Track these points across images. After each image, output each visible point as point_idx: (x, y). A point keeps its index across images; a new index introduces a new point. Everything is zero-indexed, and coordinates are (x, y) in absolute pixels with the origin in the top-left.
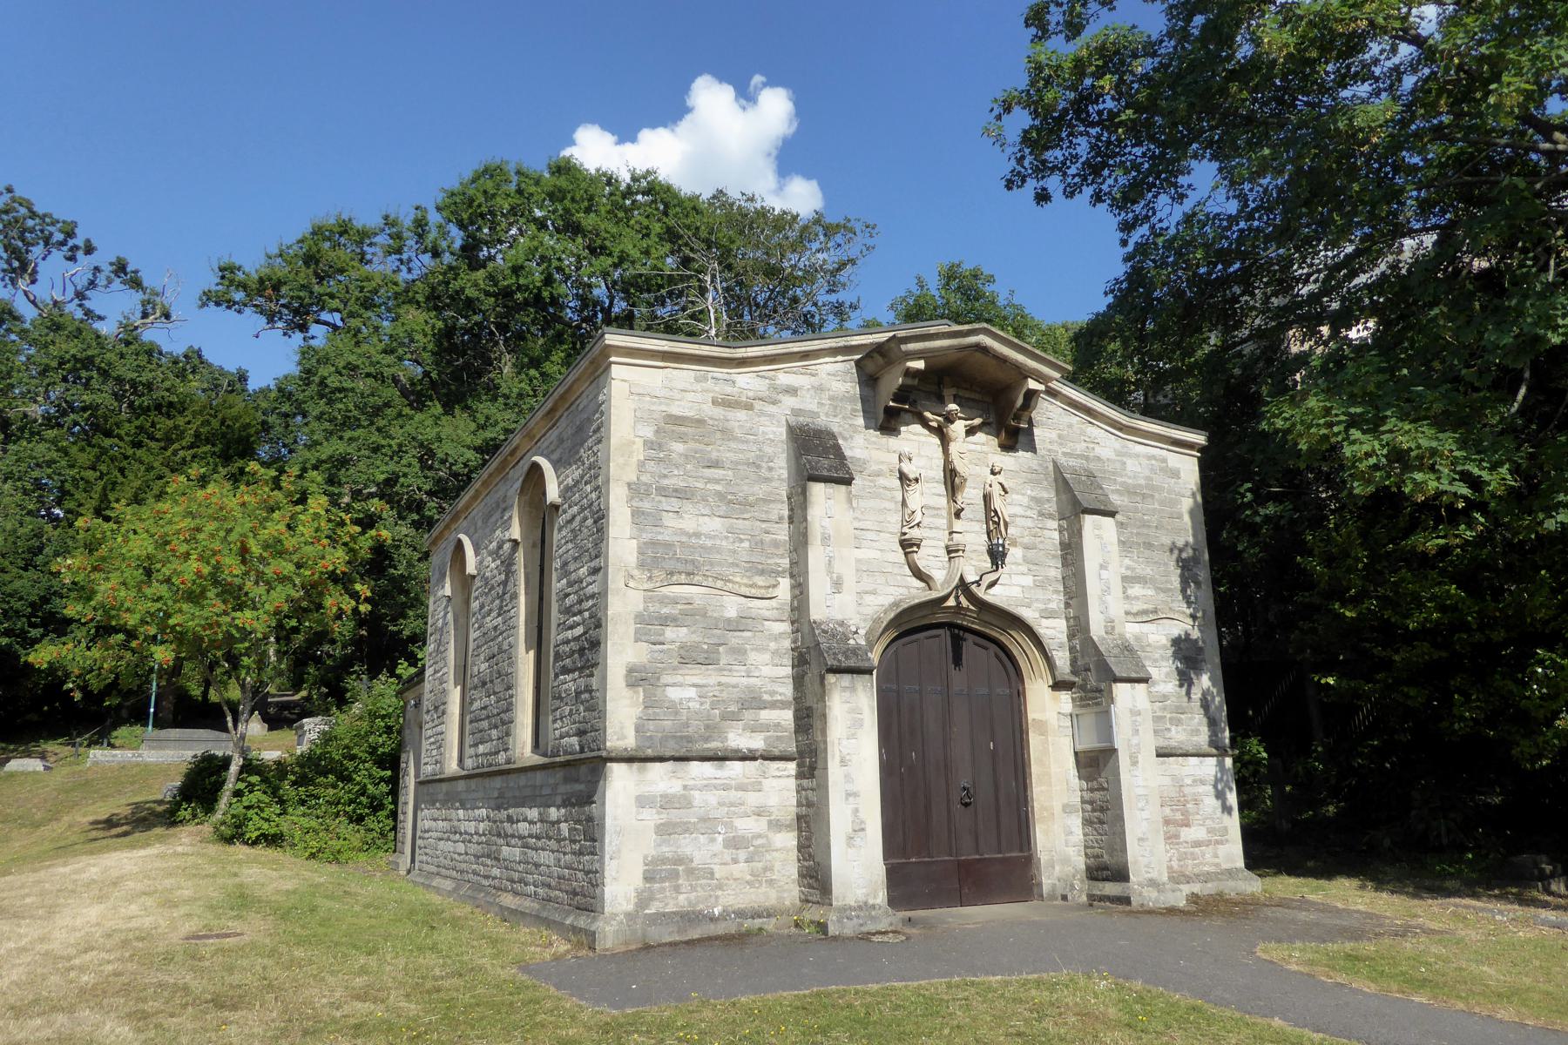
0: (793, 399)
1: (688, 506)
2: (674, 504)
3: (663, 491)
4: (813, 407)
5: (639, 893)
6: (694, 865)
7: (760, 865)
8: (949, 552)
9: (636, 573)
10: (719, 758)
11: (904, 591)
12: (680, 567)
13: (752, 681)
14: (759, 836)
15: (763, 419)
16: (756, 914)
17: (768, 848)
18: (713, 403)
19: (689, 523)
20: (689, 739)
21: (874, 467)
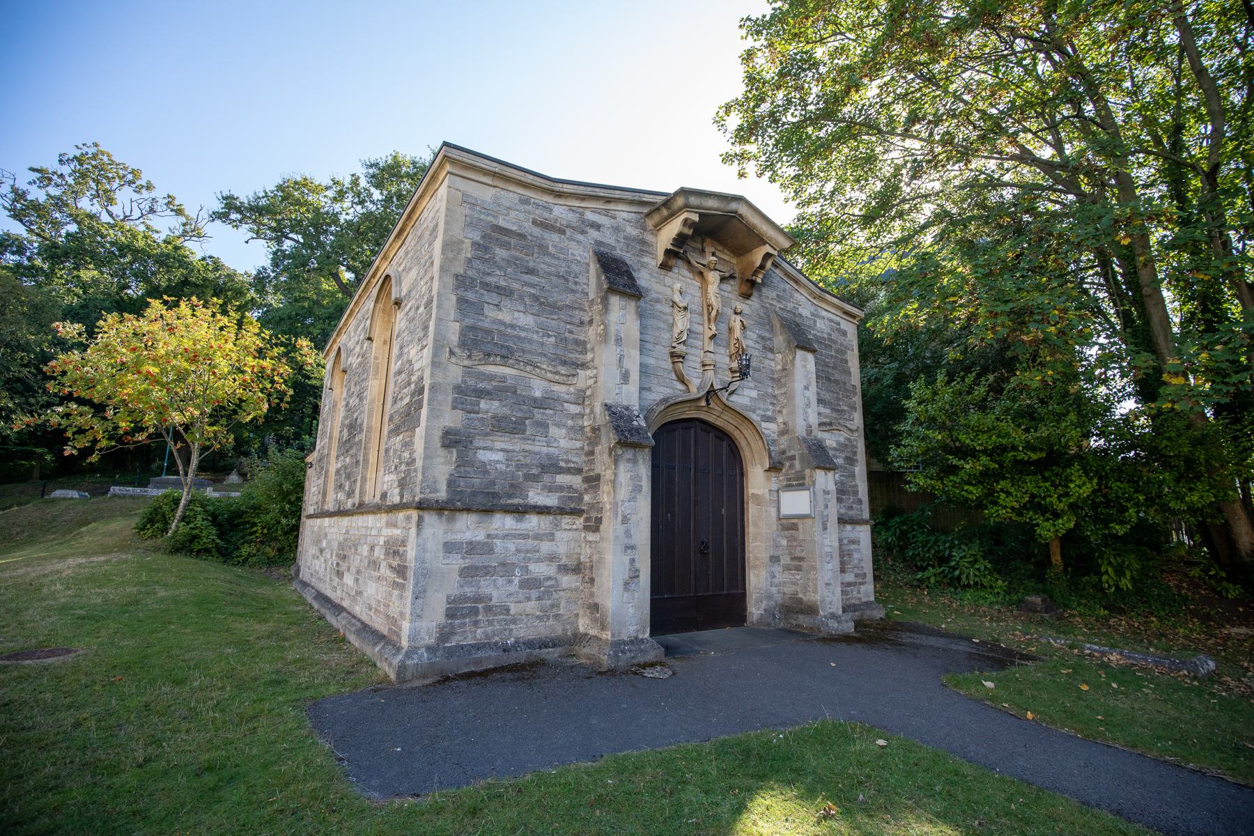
0: (597, 233)
1: (506, 302)
2: (494, 298)
3: (485, 285)
4: (612, 242)
5: (441, 628)
6: (492, 603)
7: (548, 602)
8: (704, 365)
9: (457, 350)
10: (521, 511)
11: (669, 391)
12: (496, 350)
13: (551, 450)
14: (549, 578)
15: (572, 243)
16: (544, 644)
17: (556, 587)
18: (533, 223)
19: (505, 316)
20: (495, 495)
21: (654, 295)
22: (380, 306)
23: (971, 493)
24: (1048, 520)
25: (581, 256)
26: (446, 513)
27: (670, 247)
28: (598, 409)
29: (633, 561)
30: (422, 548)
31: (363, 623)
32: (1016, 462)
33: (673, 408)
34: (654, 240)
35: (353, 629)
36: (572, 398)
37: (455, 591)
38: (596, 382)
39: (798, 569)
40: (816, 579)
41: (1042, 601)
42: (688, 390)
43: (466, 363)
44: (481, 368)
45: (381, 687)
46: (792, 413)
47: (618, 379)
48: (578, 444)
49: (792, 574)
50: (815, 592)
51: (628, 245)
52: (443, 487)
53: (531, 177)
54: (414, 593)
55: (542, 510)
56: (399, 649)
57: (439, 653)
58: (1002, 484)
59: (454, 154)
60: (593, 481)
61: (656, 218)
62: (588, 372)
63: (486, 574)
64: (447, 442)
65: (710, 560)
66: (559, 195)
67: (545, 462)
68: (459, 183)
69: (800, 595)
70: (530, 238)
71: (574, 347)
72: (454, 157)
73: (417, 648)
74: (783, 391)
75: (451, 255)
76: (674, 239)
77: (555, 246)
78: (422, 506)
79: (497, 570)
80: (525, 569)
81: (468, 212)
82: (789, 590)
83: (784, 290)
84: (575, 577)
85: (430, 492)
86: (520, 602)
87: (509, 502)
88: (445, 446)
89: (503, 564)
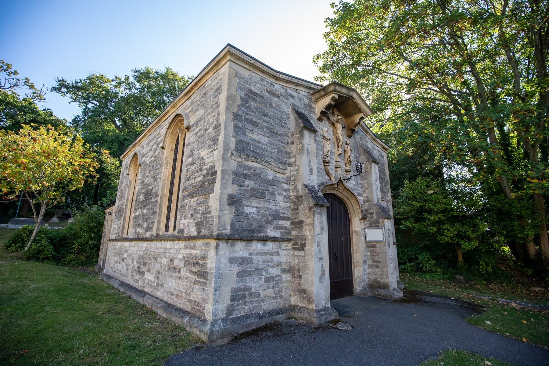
0: (292, 100)
1: (256, 129)
2: (250, 127)
3: (247, 120)
4: (298, 105)
5: (228, 307)
6: (252, 291)
7: (277, 289)
8: (336, 168)
9: (234, 152)
10: (264, 240)
11: (323, 179)
12: (252, 154)
13: (277, 207)
14: (277, 276)
15: (283, 103)
16: (277, 313)
17: (281, 281)
19: (255, 137)
20: (252, 231)
22: (170, 131)
23: (433, 230)
24: (466, 242)
25: (287, 110)
26: (230, 241)
27: (324, 110)
28: (300, 187)
29: (322, 266)
30: (219, 262)
31: (165, 302)
32: (453, 216)
33: (327, 187)
34: (315, 106)
35: (159, 306)
36: (285, 181)
37: (235, 286)
38: (297, 173)
39: (377, 267)
40: (388, 271)
41: (464, 278)
42: (330, 180)
43: (239, 159)
44: (246, 163)
45: (199, 346)
46: (371, 192)
47: (309, 172)
48: (288, 205)
49: (374, 269)
50: (387, 277)
51: (305, 108)
52: (228, 227)
53: (266, 68)
54: (215, 288)
55: (274, 240)
56: (205, 321)
57: (229, 322)
58: (445, 226)
59: (233, 51)
60: (298, 224)
61: (317, 95)
62: (292, 168)
63: (249, 275)
64: (230, 202)
65: (339, 263)
66: (277, 79)
67: (275, 214)
68: (234, 66)
69: (379, 279)
70: (265, 98)
71: (285, 155)
72: (233, 52)
73: (217, 320)
74: (366, 182)
75: (231, 102)
76: (326, 106)
77: (276, 104)
78: (219, 238)
79: (254, 273)
80: (267, 272)
81: (238, 81)
82: (372, 277)
83: (362, 135)
84: (289, 275)
85: (223, 230)
86: (265, 290)
87: (259, 235)
88: (229, 204)
89: (257, 269)
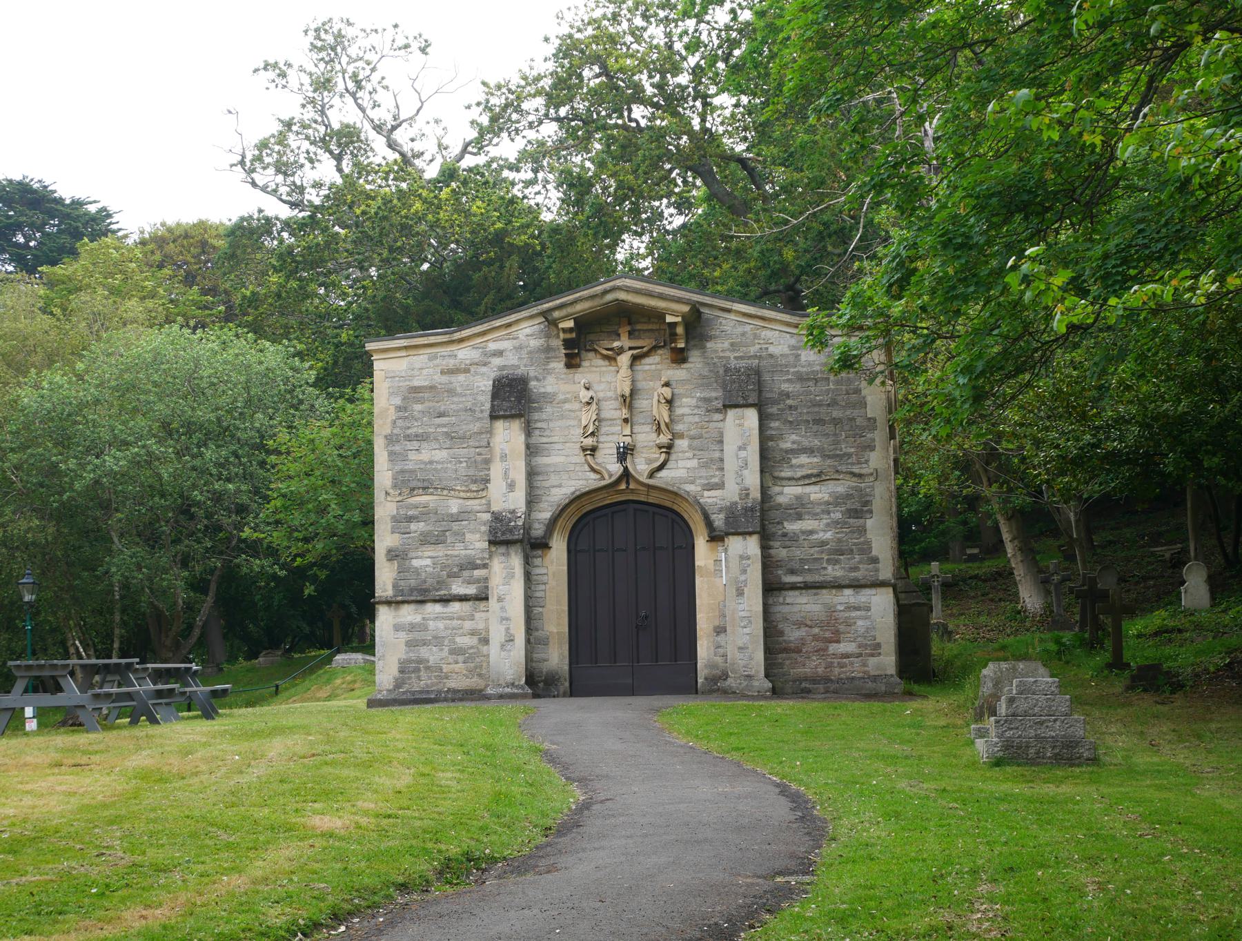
1: (424, 445)
2: (415, 444)
4: (516, 362)
5: (396, 680)
7: (472, 665)
9: (391, 491)
10: (445, 600)
12: (420, 484)
14: (472, 647)
18: (441, 373)
19: (425, 456)
20: (427, 590)
21: (561, 397)
42: (603, 478)
55: (463, 599)
64: (389, 557)
89: (435, 637)
